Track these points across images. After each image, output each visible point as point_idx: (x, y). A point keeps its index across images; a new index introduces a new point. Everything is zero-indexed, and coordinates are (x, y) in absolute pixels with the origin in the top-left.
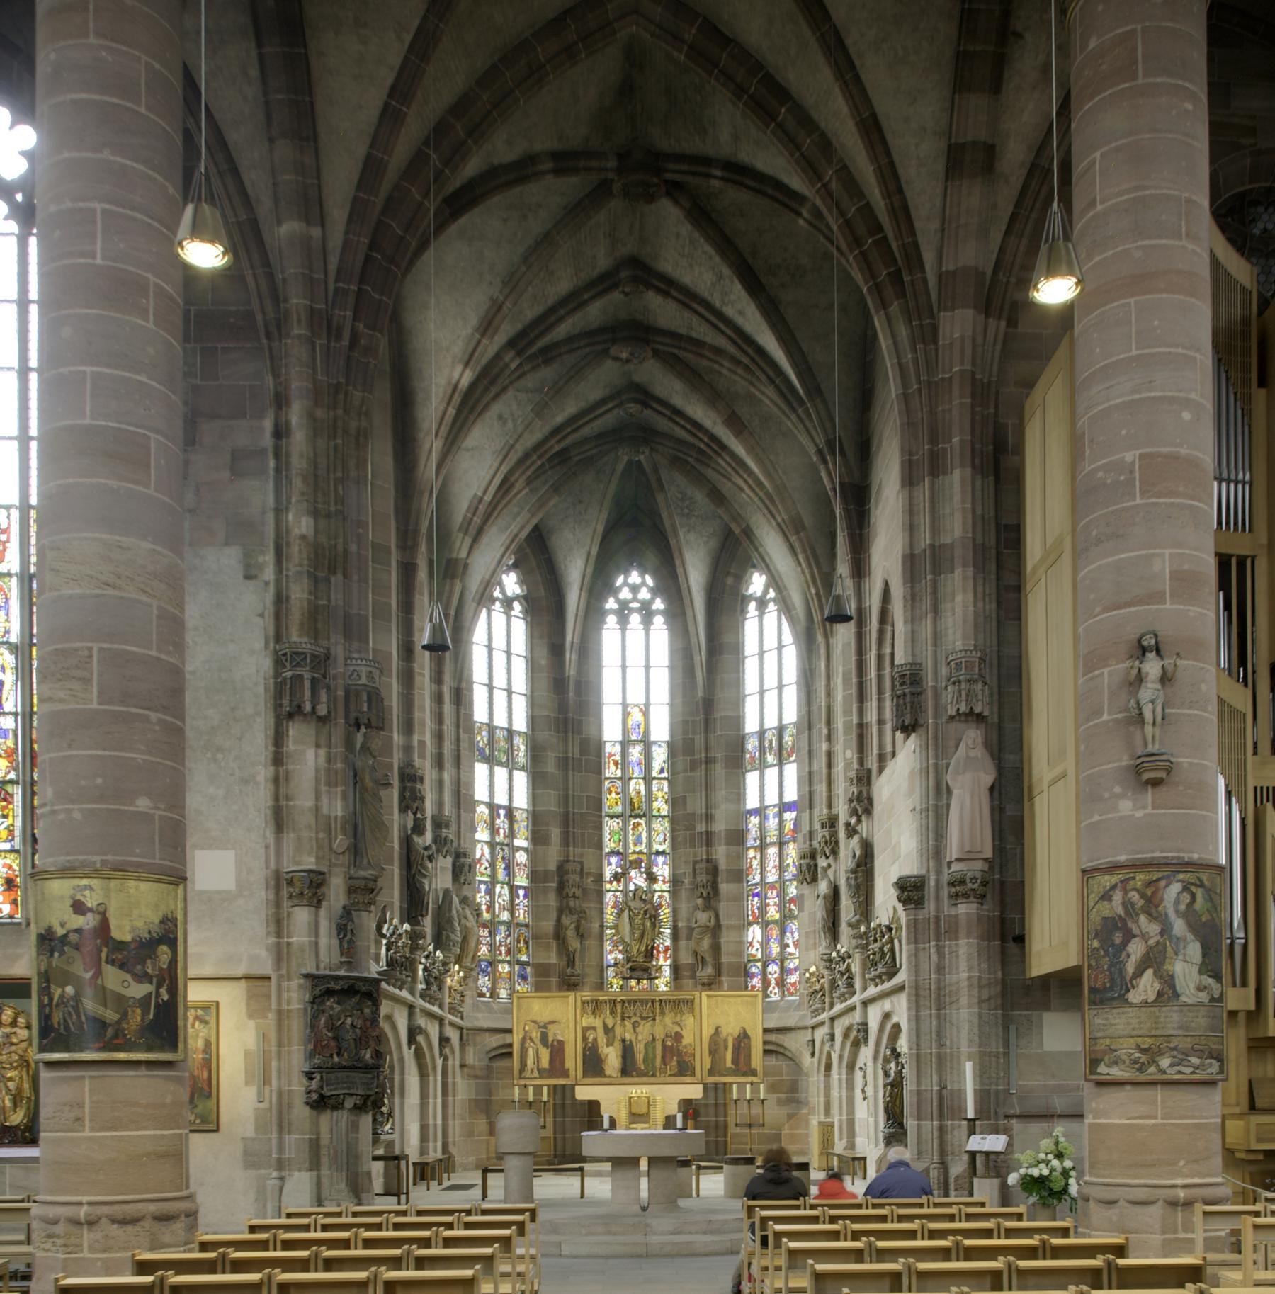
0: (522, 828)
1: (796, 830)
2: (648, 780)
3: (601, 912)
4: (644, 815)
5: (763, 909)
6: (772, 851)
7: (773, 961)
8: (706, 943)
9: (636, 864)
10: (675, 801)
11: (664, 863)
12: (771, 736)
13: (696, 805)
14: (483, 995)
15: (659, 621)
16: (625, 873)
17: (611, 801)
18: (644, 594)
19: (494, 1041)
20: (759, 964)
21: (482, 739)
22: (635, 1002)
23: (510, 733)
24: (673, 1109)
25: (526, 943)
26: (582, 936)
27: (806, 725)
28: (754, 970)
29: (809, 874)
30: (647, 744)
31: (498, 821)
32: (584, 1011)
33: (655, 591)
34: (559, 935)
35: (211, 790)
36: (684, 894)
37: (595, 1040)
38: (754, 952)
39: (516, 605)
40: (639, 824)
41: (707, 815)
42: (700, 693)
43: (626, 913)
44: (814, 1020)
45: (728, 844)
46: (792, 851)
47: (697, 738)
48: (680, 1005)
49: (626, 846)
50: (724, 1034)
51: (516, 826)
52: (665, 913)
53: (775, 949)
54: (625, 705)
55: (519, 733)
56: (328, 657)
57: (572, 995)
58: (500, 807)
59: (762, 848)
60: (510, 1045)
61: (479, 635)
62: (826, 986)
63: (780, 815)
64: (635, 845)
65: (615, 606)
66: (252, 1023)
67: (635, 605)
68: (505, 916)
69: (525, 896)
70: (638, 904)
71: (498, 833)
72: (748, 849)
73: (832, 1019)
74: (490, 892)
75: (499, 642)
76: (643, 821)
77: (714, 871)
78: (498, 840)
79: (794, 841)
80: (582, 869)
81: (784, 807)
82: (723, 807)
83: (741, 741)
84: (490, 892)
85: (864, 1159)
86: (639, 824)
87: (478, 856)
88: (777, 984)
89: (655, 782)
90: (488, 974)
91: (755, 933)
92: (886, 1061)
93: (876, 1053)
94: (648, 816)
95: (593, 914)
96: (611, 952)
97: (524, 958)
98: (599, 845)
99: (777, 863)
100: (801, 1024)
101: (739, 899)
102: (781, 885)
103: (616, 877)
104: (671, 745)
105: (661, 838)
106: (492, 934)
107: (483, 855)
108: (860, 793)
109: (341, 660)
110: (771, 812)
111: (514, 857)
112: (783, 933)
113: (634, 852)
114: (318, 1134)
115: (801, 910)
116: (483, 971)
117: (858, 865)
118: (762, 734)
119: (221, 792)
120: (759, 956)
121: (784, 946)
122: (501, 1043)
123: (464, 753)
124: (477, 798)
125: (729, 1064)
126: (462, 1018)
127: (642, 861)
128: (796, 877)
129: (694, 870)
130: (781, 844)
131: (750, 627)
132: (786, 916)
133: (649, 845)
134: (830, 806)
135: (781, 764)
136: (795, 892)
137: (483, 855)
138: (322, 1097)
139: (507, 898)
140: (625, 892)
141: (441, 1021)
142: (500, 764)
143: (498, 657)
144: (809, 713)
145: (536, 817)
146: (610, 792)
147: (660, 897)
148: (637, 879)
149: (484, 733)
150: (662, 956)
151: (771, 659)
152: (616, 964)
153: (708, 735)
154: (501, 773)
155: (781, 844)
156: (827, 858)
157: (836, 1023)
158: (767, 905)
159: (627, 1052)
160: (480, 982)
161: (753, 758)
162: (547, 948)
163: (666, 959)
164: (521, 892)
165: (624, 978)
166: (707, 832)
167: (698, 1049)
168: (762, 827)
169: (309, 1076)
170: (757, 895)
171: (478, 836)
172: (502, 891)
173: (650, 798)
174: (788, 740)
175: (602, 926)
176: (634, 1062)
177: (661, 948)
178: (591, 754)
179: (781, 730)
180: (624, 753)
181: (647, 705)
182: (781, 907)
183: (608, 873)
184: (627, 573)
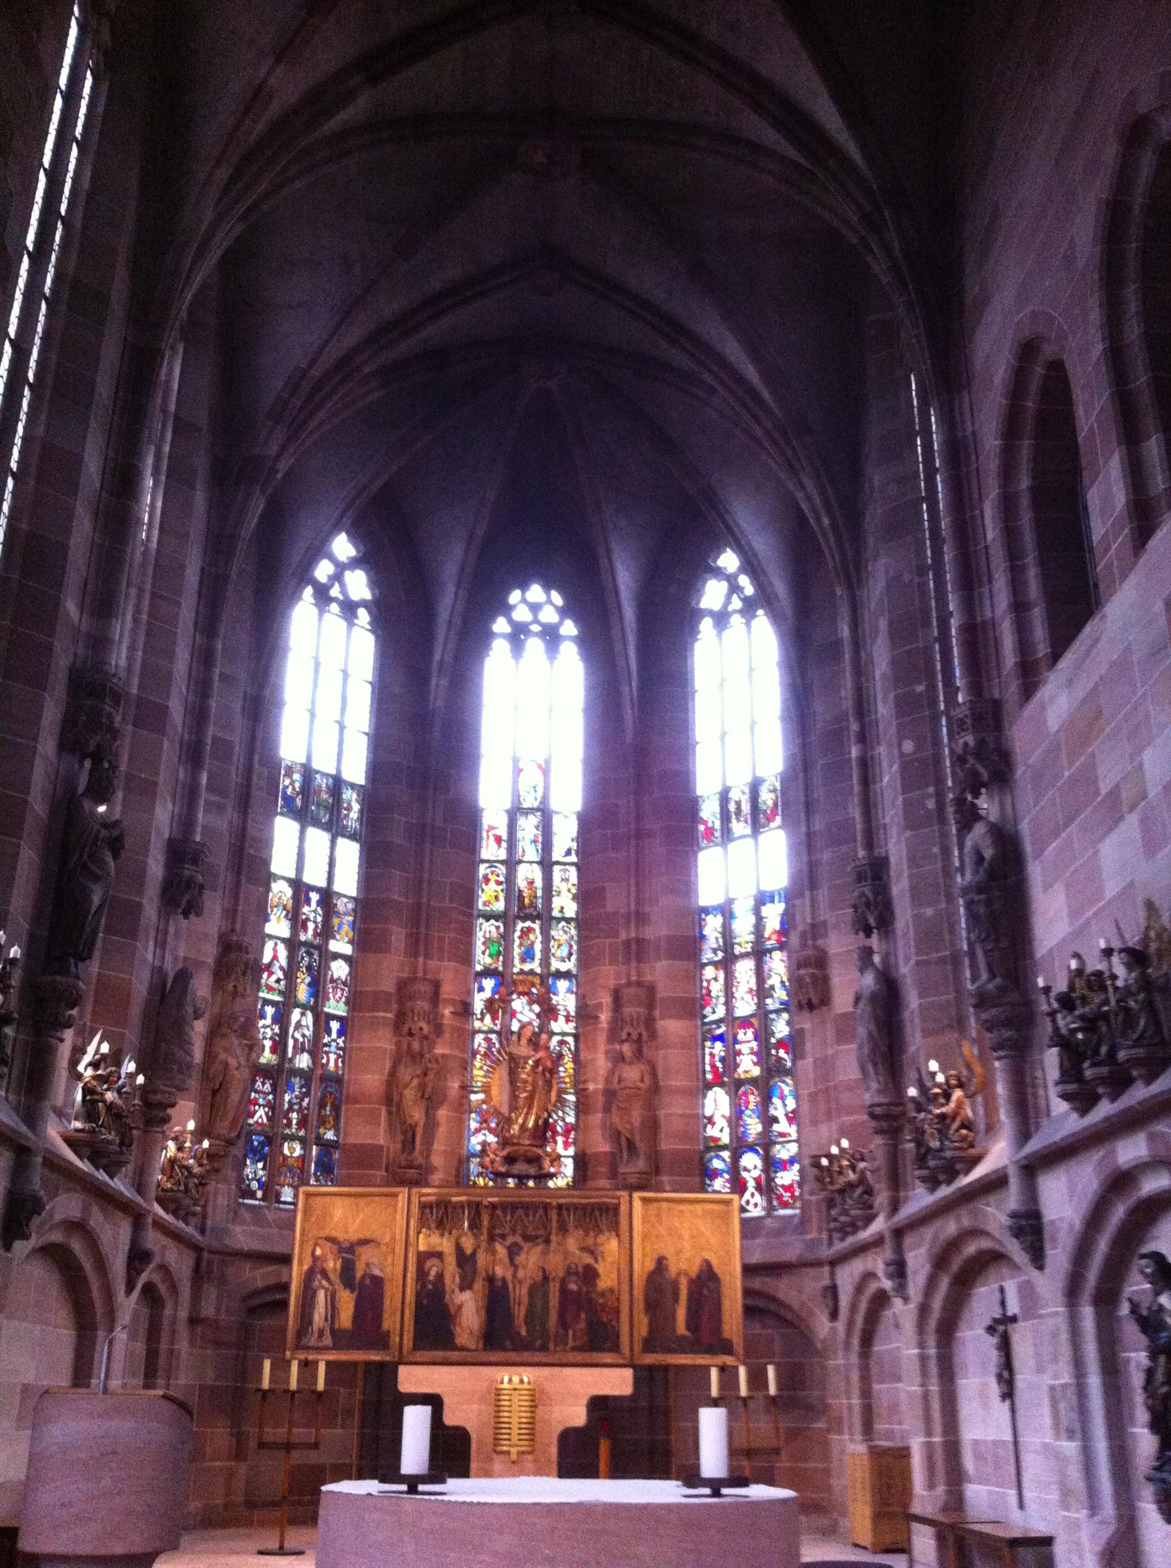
0: (345, 924)
1: (783, 932)
2: (546, 864)
3: (465, 1066)
4: (539, 916)
6: (745, 970)
7: (752, 1148)
11: (570, 991)
14: (252, 1195)
15: (570, 652)
16: (506, 1001)
17: (490, 896)
19: (258, 1276)
20: (726, 1154)
21: (290, 784)
23: (337, 784)
24: (578, 1416)
25: (336, 1109)
27: (800, 767)
28: (717, 1164)
30: (545, 814)
31: (306, 909)
32: (423, 1223)
33: (564, 612)
37: (440, 1276)
40: (530, 930)
41: (637, 913)
42: (629, 736)
44: (839, 1246)
46: (778, 966)
49: (508, 962)
50: (673, 1270)
51: (336, 921)
53: (754, 1127)
55: (353, 786)
57: (403, 1193)
59: (727, 963)
60: (285, 1287)
64: (523, 960)
65: (507, 629)
68: (303, 1061)
69: (340, 1033)
71: (305, 928)
73: (899, 1233)
74: (281, 1019)
76: (536, 926)
78: (303, 938)
79: (781, 947)
81: (762, 899)
84: (281, 1019)
87: (266, 959)
88: (759, 1188)
89: (556, 868)
90: (263, 1158)
96: (477, 1131)
97: (330, 1135)
98: (467, 958)
100: (810, 1256)
102: (761, 1021)
105: (564, 951)
107: (275, 958)
108: (981, 743)
112: (766, 1100)
113: (522, 972)
115: (797, 1056)
116: (254, 1151)
120: (725, 1139)
121: (769, 1121)
122: (272, 1281)
123: (257, 795)
124: (275, 868)
125: (681, 1328)
126: (202, 1231)
128: (786, 1007)
130: (759, 953)
132: (772, 1070)
137: (275, 958)
139: (308, 1033)
141: (138, 1219)
142: (317, 823)
143: (325, 679)
145: (369, 906)
146: (487, 880)
147: (562, 1043)
149: (297, 777)
150: (560, 1139)
152: (483, 1152)
154: (317, 838)
156: (868, 932)
157: (908, 1240)
158: (739, 1053)
159: (497, 1299)
160: (248, 1171)
162: (373, 1117)
163: (566, 1145)
164: (335, 1026)
167: (625, 1298)
168: (727, 933)
170: (721, 1038)
171: (269, 928)
172: (302, 1022)
174: (767, 798)
176: (509, 1316)
182: (763, 1055)
183: (478, 1003)
184: (524, 587)
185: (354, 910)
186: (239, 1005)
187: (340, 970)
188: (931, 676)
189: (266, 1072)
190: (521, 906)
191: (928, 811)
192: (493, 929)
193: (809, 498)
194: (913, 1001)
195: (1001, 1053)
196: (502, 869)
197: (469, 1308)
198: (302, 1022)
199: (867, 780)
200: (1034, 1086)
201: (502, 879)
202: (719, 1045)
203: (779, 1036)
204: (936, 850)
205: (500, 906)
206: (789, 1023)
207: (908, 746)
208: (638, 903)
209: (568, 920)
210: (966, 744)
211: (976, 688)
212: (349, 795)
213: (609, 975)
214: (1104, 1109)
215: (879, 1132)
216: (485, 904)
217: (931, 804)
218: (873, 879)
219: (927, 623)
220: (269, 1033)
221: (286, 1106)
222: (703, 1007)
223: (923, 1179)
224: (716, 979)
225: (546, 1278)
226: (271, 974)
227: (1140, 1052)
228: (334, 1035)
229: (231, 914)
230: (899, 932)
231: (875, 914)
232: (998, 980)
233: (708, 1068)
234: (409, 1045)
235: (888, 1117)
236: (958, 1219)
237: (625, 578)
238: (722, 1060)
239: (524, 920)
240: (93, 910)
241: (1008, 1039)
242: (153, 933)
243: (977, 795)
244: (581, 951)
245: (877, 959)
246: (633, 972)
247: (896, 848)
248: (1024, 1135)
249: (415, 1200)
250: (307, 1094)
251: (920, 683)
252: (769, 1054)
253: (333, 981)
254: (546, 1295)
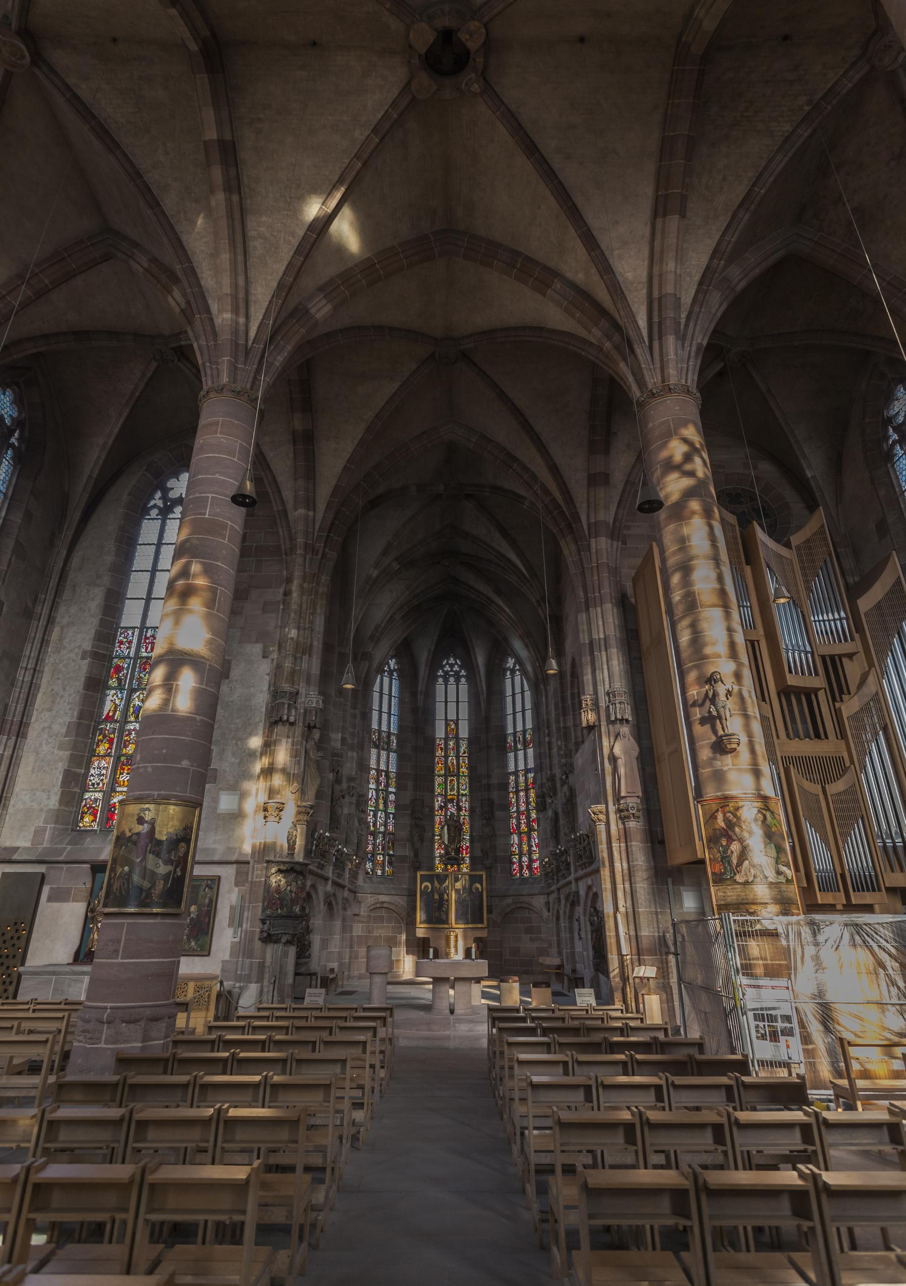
0: (393, 782)
9: (451, 801)
16: (446, 805)
17: (439, 769)
18: (456, 668)
21: (374, 737)
23: (389, 734)
30: (457, 739)
33: (461, 667)
35: (233, 760)
39: (395, 674)
54: (446, 720)
56: (297, 693)
58: (382, 771)
61: (377, 687)
63: (525, 775)
66: (236, 889)
75: (386, 690)
77: (491, 802)
83: (504, 737)
85: (583, 978)
92: (591, 915)
93: (585, 910)
98: (433, 791)
103: (441, 808)
104: (471, 741)
109: (304, 695)
114: (264, 958)
118: (515, 733)
119: (238, 761)
131: (508, 682)
133: (458, 791)
134: (551, 770)
135: (525, 749)
138: (269, 935)
140: (446, 815)
142: (383, 749)
144: (538, 723)
151: (518, 697)
154: (384, 754)
161: (511, 746)
169: (263, 922)
178: (429, 744)
179: (524, 731)
180: (446, 744)
181: (458, 719)
183: (437, 805)
184: (448, 659)
187: (392, 797)
205: (443, 772)
212: (393, 738)
237: (481, 659)
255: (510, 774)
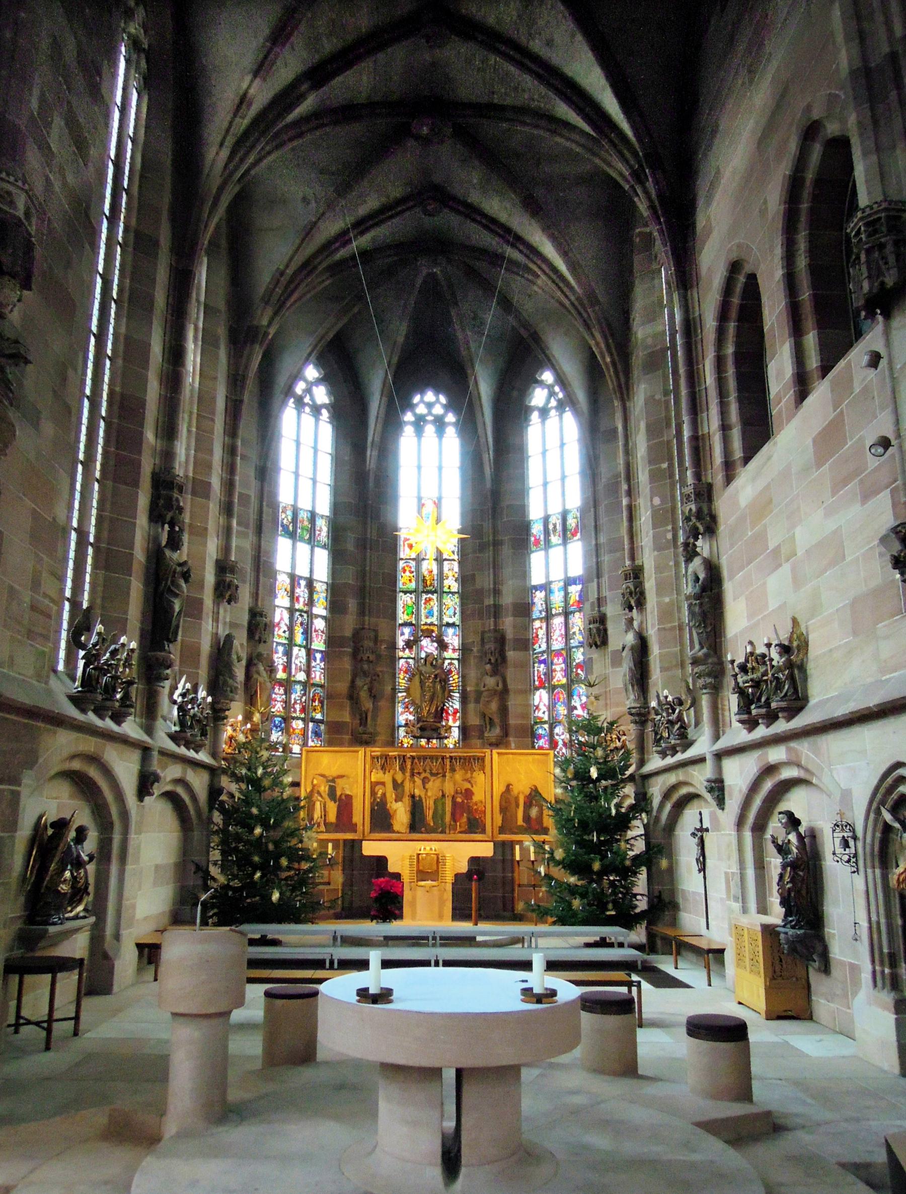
1: (580, 602)
4: (435, 592)
5: (549, 674)
6: (558, 622)
8: (494, 706)
9: (428, 634)
10: (464, 579)
11: (454, 634)
12: (556, 520)
13: (485, 581)
22: (425, 758)
25: (321, 702)
26: (375, 697)
27: (592, 503)
28: (540, 731)
29: (598, 636)
33: (447, 407)
34: (353, 696)
36: (472, 661)
38: (540, 714)
40: (430, 599)
41: (494, 589)
43: (417, 677)
45: (514, 615)
46: (578, 621)
47: (485, 525)
48: (473, 763)
51: (315, 597)
52: (455, 679)
58: (301, 578)
59: (548, 618)
62: (631, 746)
63: (565, 589)
64: (427, 618)
67: (430, 418)
68: (301, 676)
69: (321, 660)
70: (427, 669)
72: (534, 620)
74: (288, 653)
76: (434, 597)
77: (501, 640)
78: (297, 606)
80: (376, 637)
82: (510, 582)
84: (288, 653)
86: (430, 599)
87: (277, 620)
89: (445, 563)
91: (541, 698)
94: (440, 592)
95: (387, 677)
96: (402, 713)
97: (319, 716)
98: (394, 616)
99: (563, 632)
101: (525, 667)
103: (409, 645)
105: (451, 612)
106: (288, 692)
107: (282, 619)
110: (555, 587)
111: (312, 623)
112: (570, 696)
113: (426, 624)
117: (704, 589)
120: (546, 718)
127: (433, 631)
128: (581, 644)
129: (483, 639)
130: (567, 614)
133: (441, 618)
135: (565, 542)
136: (582, 658)
137: (282, 619)
139: (304, 661)
140: (417, 659)
146: (404, 571)
147: (450, 664)
148: (428, 646)
150: (451, 718)
153: (496, 526)
155: (567, 614)
156: (630, 608)
162: (341, 707)
164: (318, 656)
165: (414, 737)
166: (495, 605)
168: (547, 601)
170: (544, 662)
171: (277, 602)
172: (299, 655)
173: (441, 576)
175: (394, 690)
177: (451, 711)
182: (568, 672)
185: (327, 590)
186: (261, 648)
188: (671, 459)
189: (280, 683)
190: (425, 585)
191: (668, 541)
192: (409, 599)
193: (597, 344)
194: (655, 650)
195: (704, 691)
196: (413, 564)
197: (401, 813)
198: (299, 655)
199: (631, 519)
200: (723, 710)
201: (413, 569)
202: (542, 666)
203: (577, 661)
204: (672, 563)
206: (583, 654)
207: (657, 501)
208: (495, 583)
209: (453, 593)
210: (691, 510)
211: (698, 476)
213: (476, 624)
214: (761, 731)
215: (636, 722)
216: (404, 584)
217: (669, 536)
218: (634, 578)
219: (668, 425)
220: (281, 662)
221: (293, 702)
222: (534, 644)
223: (658, 752)
224: (541, 628)
225: (443, 796)
226: (279, 629)
227: (783, 704)
228: (318, 661)
229: (255, 595)
230: (648, 610)
231: (636, 599)
232: (705, 650)
233: (536, 678)
234: (362, 668)
235: (638, 714)
236: (677, 775)
238: (545, 674)
239: (428, 592)
240: (176, 614)
241: (710, 683)
242: (211, 614)
243: (696, 539)
244: (463, 613)
245: (636, 624)
246: (492, 623)
247: (648, 560)
248: (717, 737)
249: (368, 754)
250: (305, 694)
251: (664, 463)
252: (572, 671)
253: (316, 631)
254: (444, 804)
255: (536, 588)
